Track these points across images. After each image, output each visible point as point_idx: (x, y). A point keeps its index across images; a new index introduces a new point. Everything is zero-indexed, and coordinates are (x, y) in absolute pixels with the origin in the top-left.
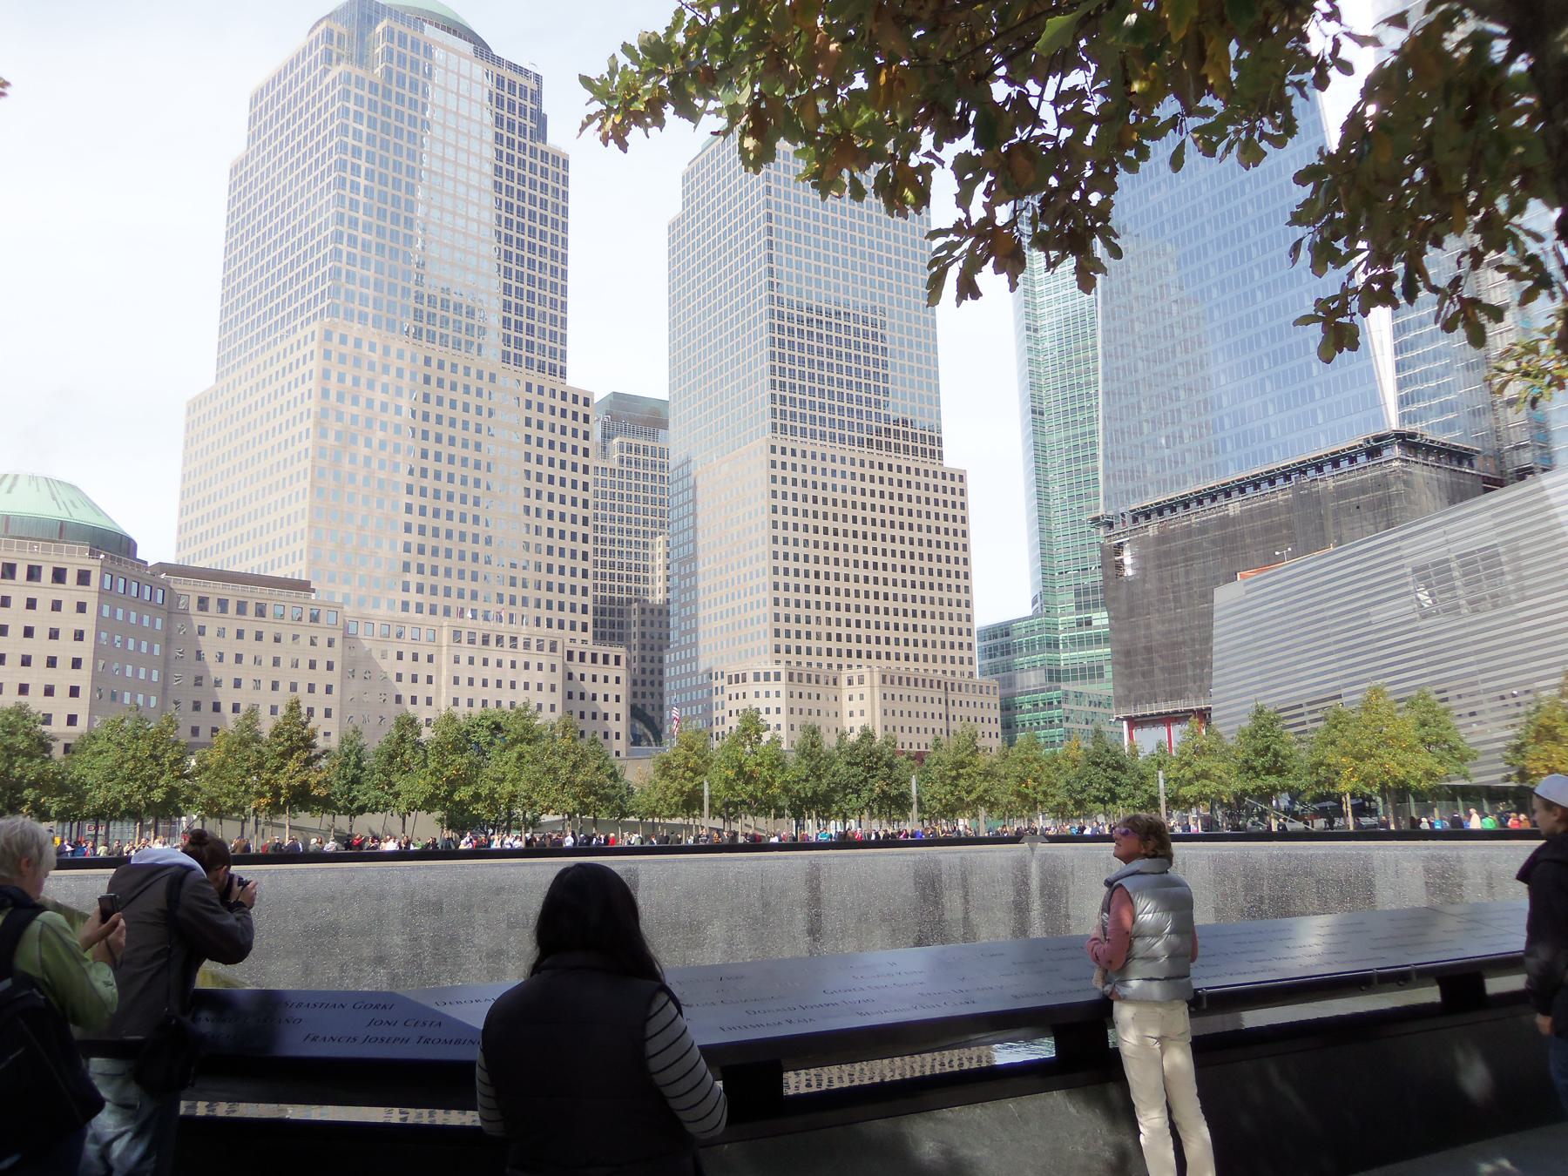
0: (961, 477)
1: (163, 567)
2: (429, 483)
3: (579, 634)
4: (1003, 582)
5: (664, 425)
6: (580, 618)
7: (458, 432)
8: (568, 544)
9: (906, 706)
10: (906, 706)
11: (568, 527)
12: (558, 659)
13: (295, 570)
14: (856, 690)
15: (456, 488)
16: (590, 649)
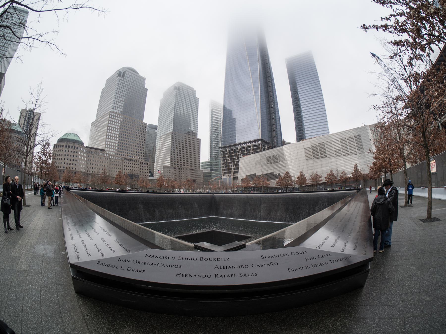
0: (200, 140)
1: (87, 147)
2: (122, 136)
3: (142, 160)
4: (205, 156)
5: (156, 129)
6: (143, 157)
7: (127, 128)
8: (141, 146)
9: (190, 173)
10: (190, 173)
11: (142, 143)
12: (139, 163)
13: (102, 147)
14: (182, 170)
15: (126, 137)
16: (144, 162)
